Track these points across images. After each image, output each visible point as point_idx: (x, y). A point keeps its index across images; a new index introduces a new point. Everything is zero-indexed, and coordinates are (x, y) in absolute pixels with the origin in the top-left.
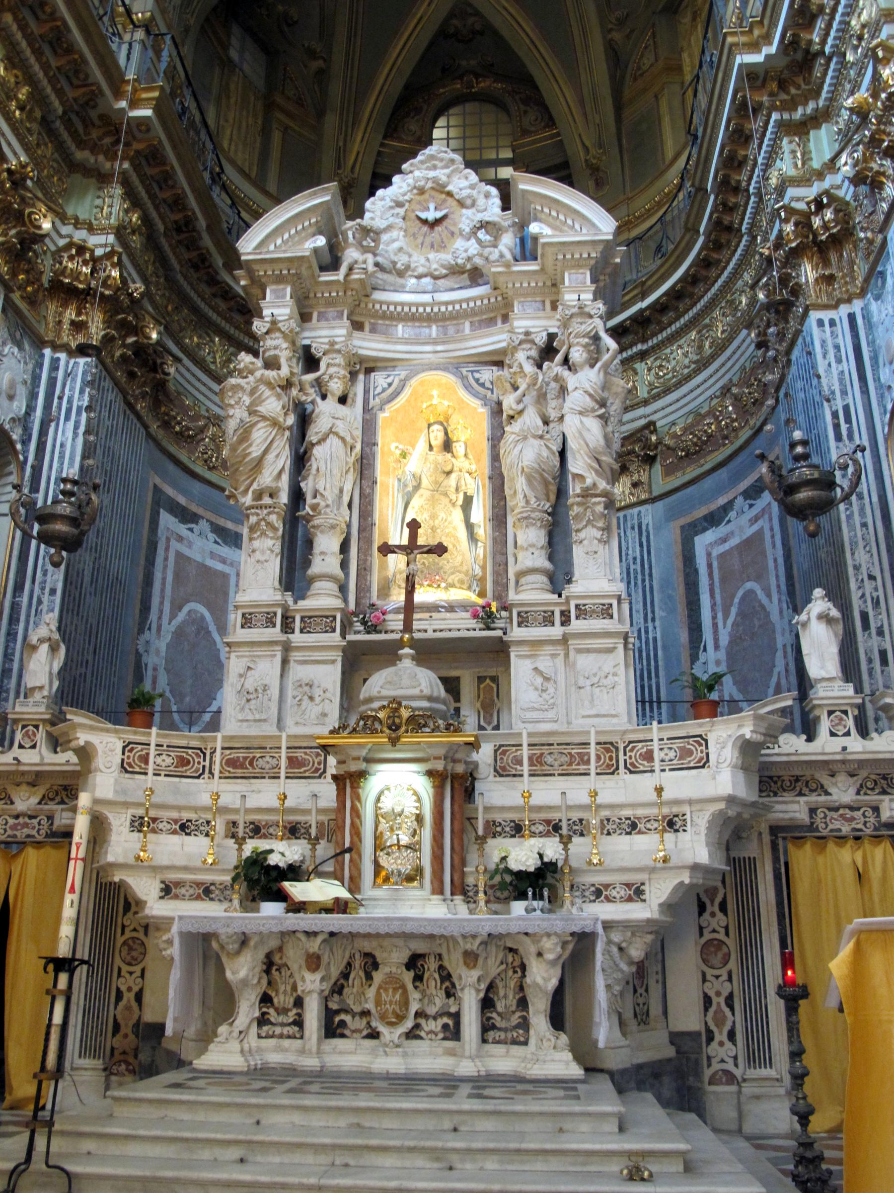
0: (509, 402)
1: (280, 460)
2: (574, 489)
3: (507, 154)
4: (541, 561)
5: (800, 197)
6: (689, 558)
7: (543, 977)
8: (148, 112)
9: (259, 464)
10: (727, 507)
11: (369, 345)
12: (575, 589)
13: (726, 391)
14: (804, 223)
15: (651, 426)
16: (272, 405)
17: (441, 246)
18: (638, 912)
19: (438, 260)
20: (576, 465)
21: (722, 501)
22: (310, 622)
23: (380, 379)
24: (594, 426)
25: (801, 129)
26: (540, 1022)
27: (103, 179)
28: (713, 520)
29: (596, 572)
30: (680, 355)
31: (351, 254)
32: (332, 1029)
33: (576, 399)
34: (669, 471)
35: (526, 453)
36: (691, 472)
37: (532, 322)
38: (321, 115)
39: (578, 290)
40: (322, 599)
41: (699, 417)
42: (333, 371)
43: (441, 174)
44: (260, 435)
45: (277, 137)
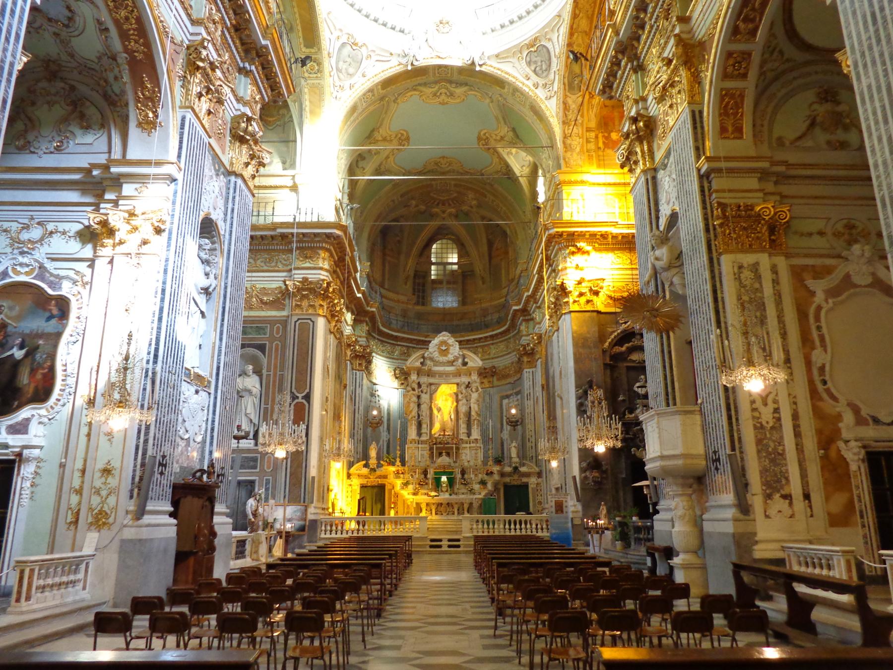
0: (460, 397)
1: (416, 409)
2: (473, 418)
3: (455, 260)
4: (465, 431)
5: (524, 340)
6: (501, 406)
7: (466, 506)
8: (374, 310)
9: (411, 412)
10: (511, 395)
11: (432, 380)
12: (472, 438)
13: (512, 363)
14: (525, 348)
15: (494, 367)
16: (415, 399)
17: (446, 356)
18: (480, 497)
19: (444, 359)
20: (473, 413)
21: (509, 393)
22: (423, 442)
23: (433, 387)
24: (476, 406)
25: (527, 321)
26: (466, 512)
27: (361, 322)
28: (508, 397)
29: (476, 434)
30: (502, 346)
31: (428, 362)
32: (436, 514)
33: (473, 400)
34: (498, 380)
35: (463, 409)
36: (504, 382)
37: (465, 380)
38: (399, 253)
39: (475, 377)
40: (424, 438)
41: (506, 368)
42: (424, 387)
43: (445, 338)
44: (412, 405)
45: (387, 265)
